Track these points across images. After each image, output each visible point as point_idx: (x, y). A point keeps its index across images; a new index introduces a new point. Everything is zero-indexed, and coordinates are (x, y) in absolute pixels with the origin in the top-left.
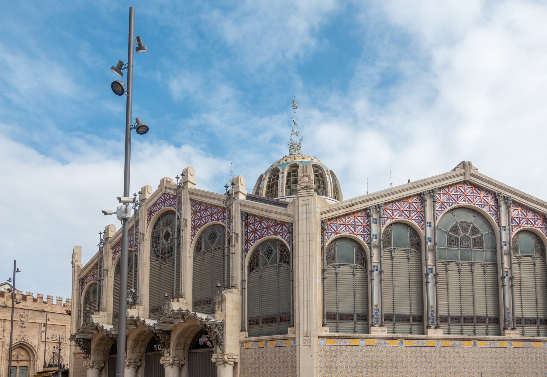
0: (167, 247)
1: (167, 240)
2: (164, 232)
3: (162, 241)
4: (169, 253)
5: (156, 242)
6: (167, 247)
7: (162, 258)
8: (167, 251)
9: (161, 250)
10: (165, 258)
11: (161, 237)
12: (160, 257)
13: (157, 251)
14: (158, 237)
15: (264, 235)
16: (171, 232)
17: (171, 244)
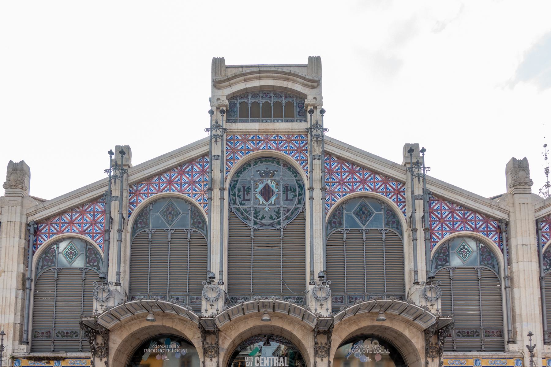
0: (267, 209)
1: (267, 199)
2: (261, 187)
3: (256, 198)
4: (271, 218)
5: (242, 197)
6: (267, 209)
7: (255, 223)
8: (267, 216)
9: (252, 209)
10: (263, 225)
11: (252, 192)
12: (252, 221)
13: (245, 210)
14: (247, 190)
15: (459, 229)
16: (277, 188)
17: (277, 206)
